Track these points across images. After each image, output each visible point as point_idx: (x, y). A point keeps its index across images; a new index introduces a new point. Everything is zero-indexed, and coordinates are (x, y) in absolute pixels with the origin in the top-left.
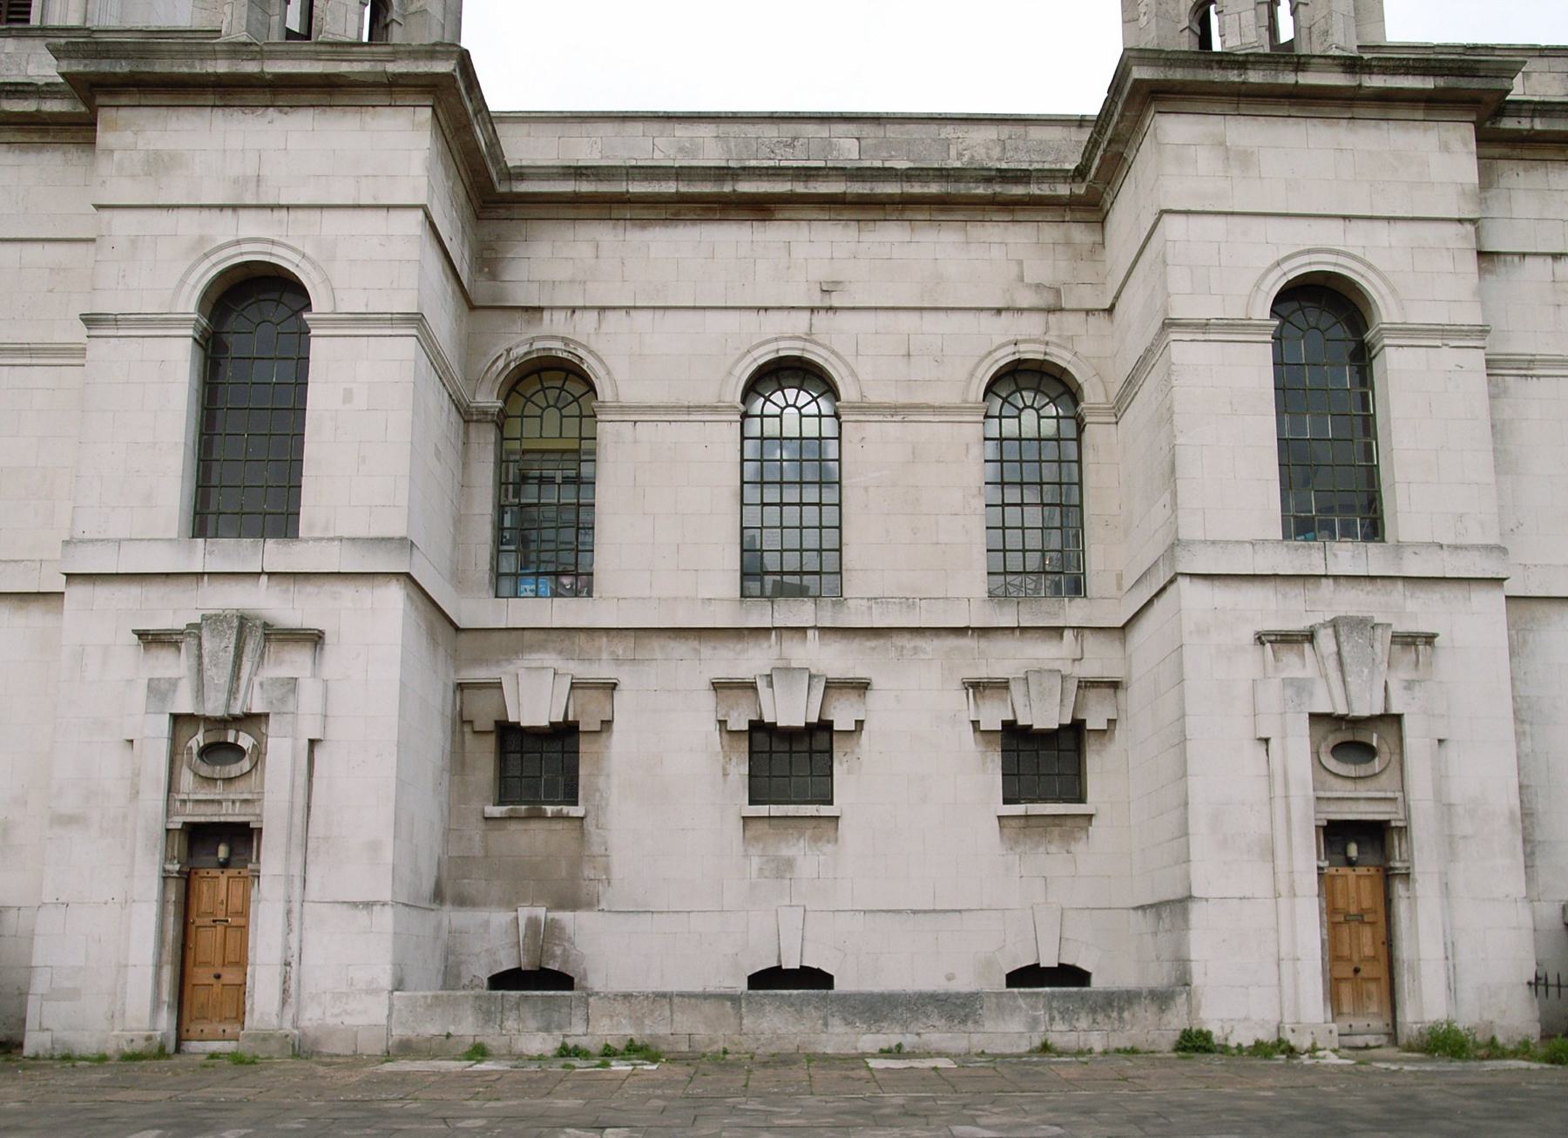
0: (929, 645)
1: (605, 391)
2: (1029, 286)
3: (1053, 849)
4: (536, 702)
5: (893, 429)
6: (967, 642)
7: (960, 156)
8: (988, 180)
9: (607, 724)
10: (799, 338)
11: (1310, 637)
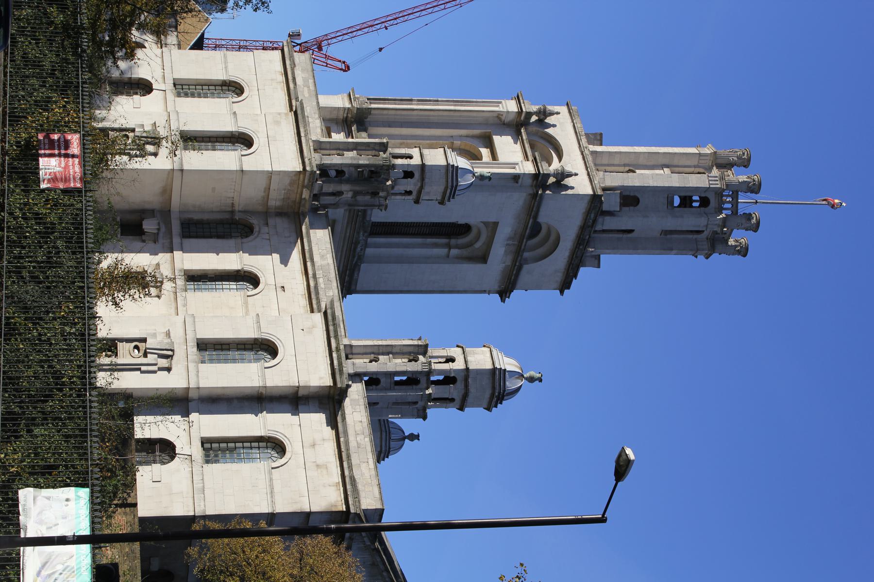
1: (245, 240)
4: (149, 226)
9: (144, 241)
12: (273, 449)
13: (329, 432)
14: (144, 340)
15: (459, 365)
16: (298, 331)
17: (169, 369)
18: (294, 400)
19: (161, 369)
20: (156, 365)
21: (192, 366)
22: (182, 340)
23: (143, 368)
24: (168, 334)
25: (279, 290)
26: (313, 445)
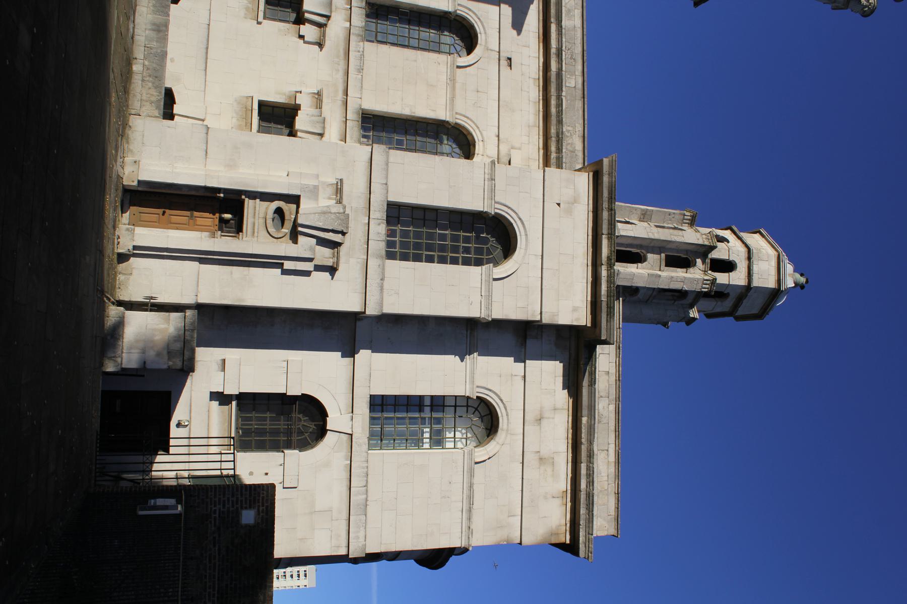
0: (340, 76)
2: (509, 151)
3: (234, 120)
5: (444, 78)
6: (340, 95)
7: (568, 131)
8: (558, 136)
10: (486, 42)
11: (340, 202)
12: (482, 418)
13: (562, 398)
14: (295, 200)
15: (737, 278)
16: (551, 206)
17: (332, 270)
18: (522, 338)
19: (318, 268)
20: (310, 260)
21: (373, 263)
22: (363, 203)
23: (288, 265)
24: (339, 189)
25: (504, 63)
26: (539, 420)
